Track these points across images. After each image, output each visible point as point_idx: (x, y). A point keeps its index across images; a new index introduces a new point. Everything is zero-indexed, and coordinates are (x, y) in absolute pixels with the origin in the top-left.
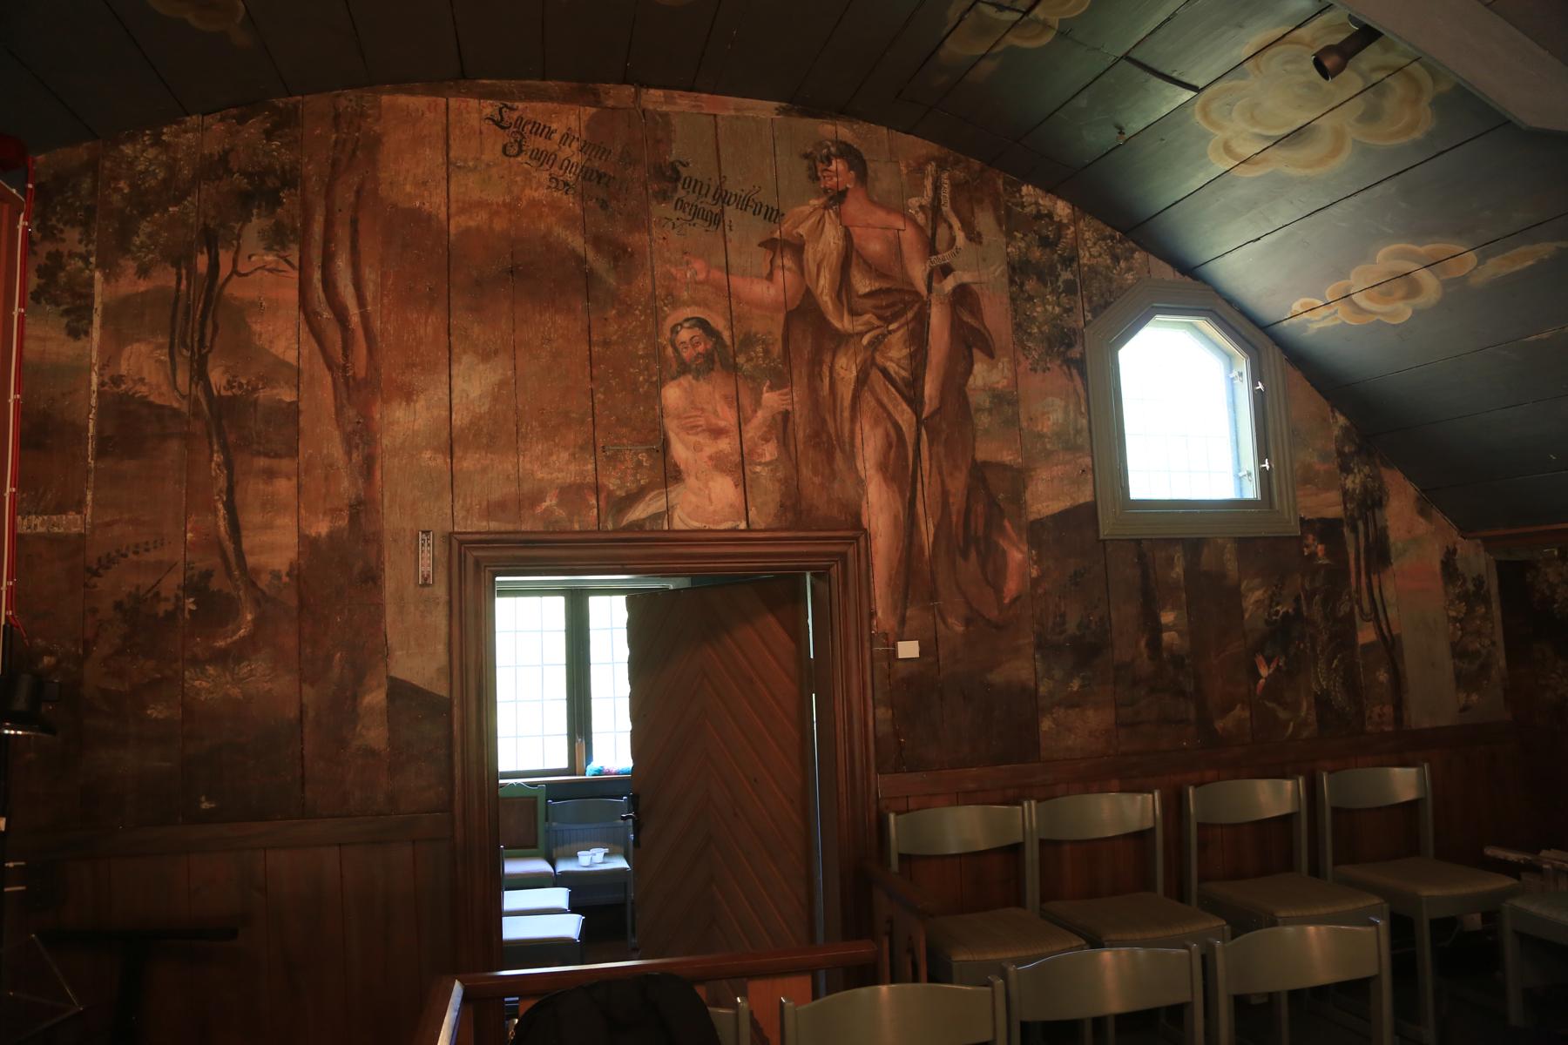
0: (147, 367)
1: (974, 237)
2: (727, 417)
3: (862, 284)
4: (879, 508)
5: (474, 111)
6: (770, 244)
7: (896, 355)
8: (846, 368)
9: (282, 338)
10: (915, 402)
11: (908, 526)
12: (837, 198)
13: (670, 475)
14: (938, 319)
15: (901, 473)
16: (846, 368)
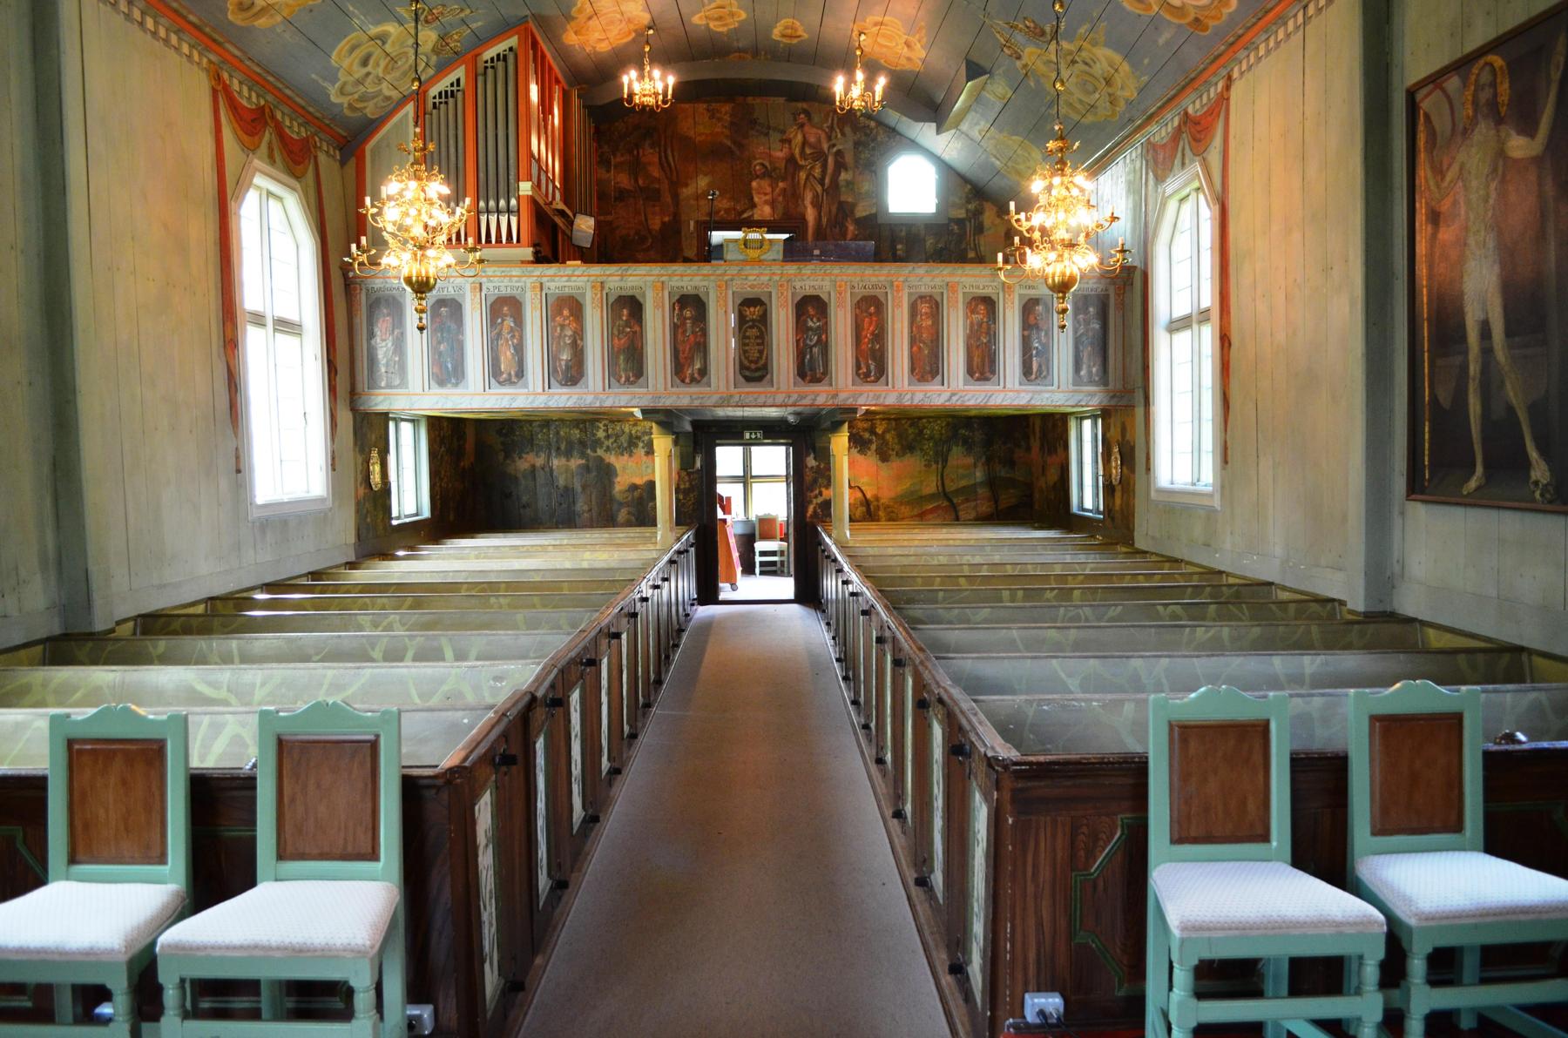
0: (624, 180)
1: (843, 134)
2: (769, 190)
3: (808, 151)
4: (810, 214)
5: (702, 107)
6: (782, 141)
7: (817, 172)
8: (803, 175)
9: (656, 172)
10: (822, 185)
11: (819, 219)
12: (802, 126)
13: (754, 206)
14: (831, 160)
15: (817, 205)
16: (803, 175)
